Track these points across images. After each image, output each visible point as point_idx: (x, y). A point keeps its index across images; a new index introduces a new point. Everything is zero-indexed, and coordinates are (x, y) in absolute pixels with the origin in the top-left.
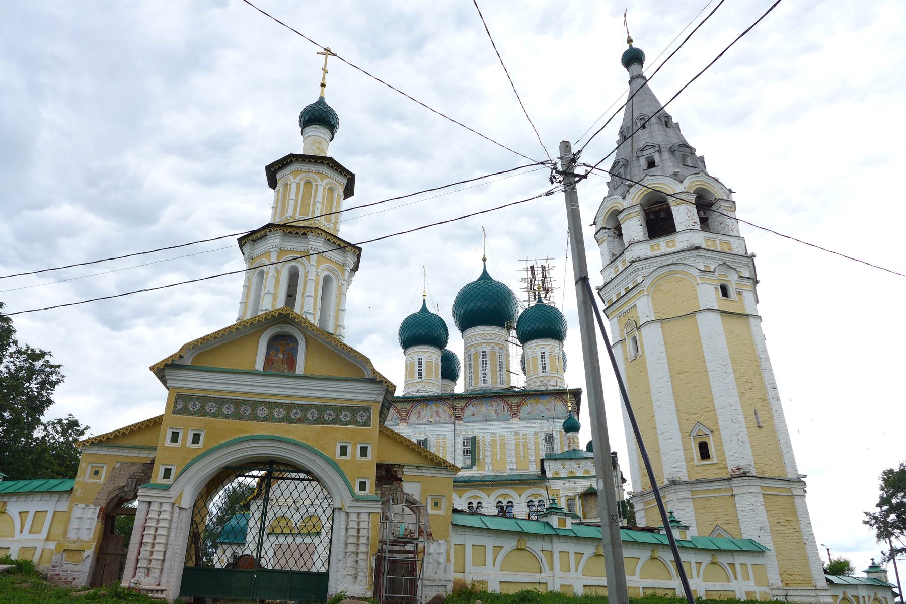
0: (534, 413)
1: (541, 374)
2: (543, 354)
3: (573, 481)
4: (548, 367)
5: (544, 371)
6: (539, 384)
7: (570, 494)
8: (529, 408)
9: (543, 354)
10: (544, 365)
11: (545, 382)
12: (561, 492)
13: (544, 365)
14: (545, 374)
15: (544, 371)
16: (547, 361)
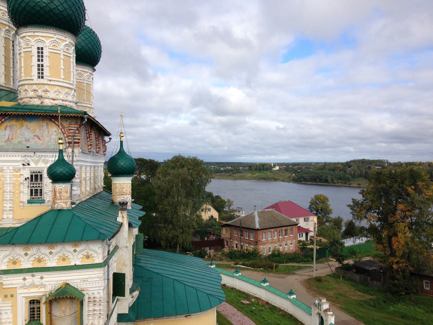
0: (16, 141)
1: (36, 80)
2: (40, 50)
3: (38, 275)
4: (46, 72)
5: (41, 76)
6: (31, 94)
7: (35, 293)
8: (8, 132)
9: (40, 50)
10: (41, 68)
11: (40, 93)
12: (19, 291)
13: (41, 68)
14: (41, 81)
15: (41, 76)
16: (46, 62)
